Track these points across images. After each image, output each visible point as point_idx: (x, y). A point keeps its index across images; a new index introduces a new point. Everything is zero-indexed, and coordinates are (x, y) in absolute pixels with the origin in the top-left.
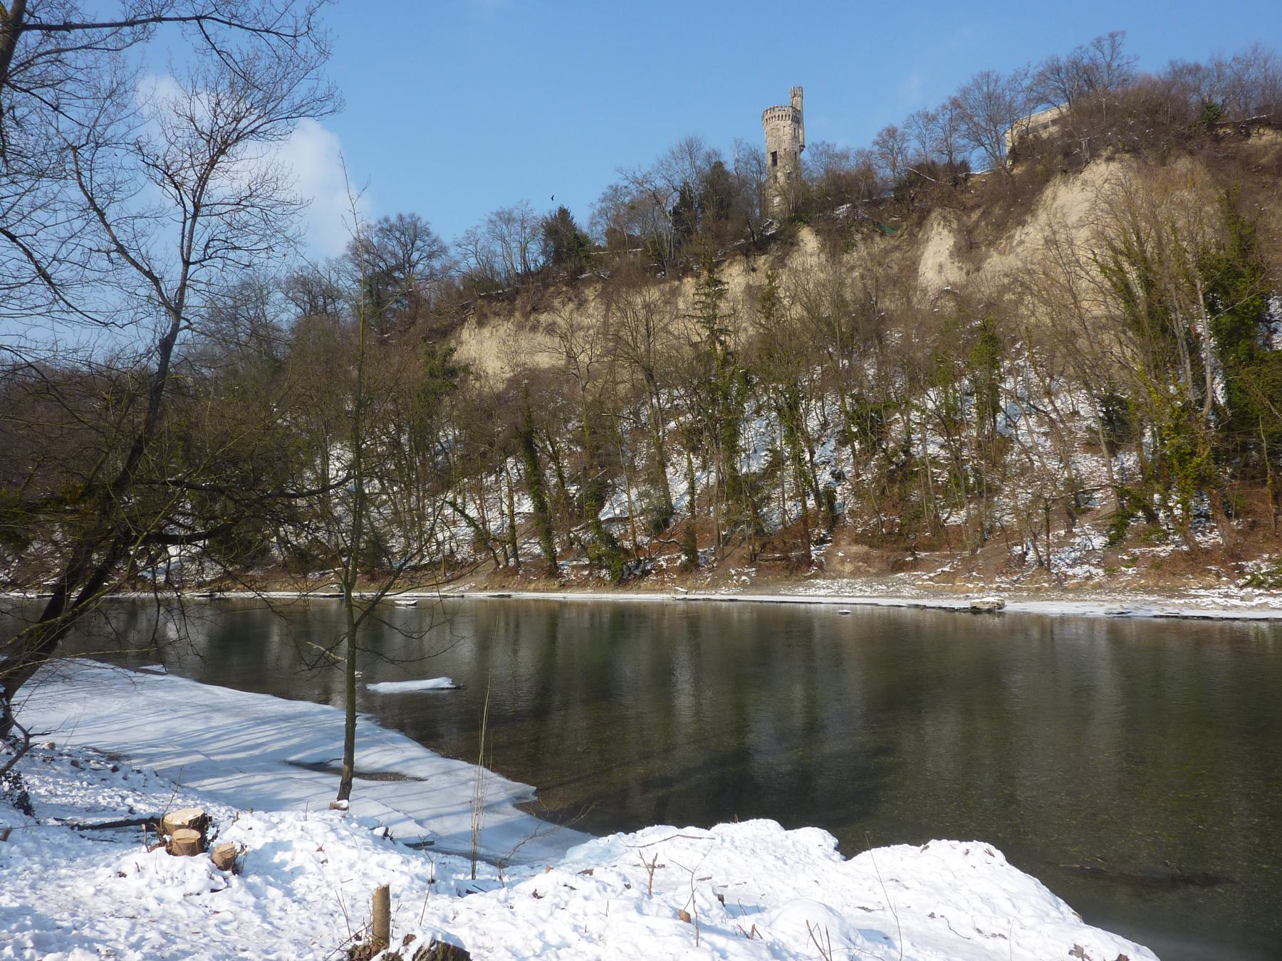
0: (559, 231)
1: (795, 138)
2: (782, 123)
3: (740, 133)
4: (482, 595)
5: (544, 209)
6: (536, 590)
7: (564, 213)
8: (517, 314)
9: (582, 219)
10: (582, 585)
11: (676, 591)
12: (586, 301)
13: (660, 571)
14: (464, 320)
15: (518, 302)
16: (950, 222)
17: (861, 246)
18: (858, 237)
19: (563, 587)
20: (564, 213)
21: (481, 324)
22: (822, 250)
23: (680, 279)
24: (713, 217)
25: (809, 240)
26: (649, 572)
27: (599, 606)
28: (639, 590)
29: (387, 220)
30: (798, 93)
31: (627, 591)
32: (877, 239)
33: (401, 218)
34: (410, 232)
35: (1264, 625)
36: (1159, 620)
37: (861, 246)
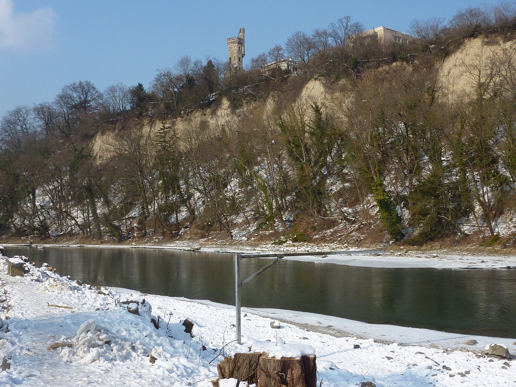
0: (138, 92)
1: (239, 50)
2: (233, 45)
3: (213, 49)
4: (75, 246)
5: (131, 83)
6: (94, 244)
7: (140, 86)
8: (117, 130)
9: (148, 88)
10: (108, 242)
11: (132, 245)
12: (143, 125)
13: (134, 237)
14: (97, 132)
15: (117, 125)
16: (274, 98)
17: (245, 105)
18: (244, 102)
19: (102, 243)
20: (140, 86)
21: (103, 134)
22: (229, 107)
23: (176, 118)
24: (197, 89)
25: (226, 103)
26: (130, 238)
27: (113, 250)
28: (125, 244)
29: (74, 84)
30: (242, 31)
31: (121, 245)
32: (253, 102)
33: (81, 83)
34: (85, 88)
35: (134, 250)
36: (465, 270)
37: (245, 105)
